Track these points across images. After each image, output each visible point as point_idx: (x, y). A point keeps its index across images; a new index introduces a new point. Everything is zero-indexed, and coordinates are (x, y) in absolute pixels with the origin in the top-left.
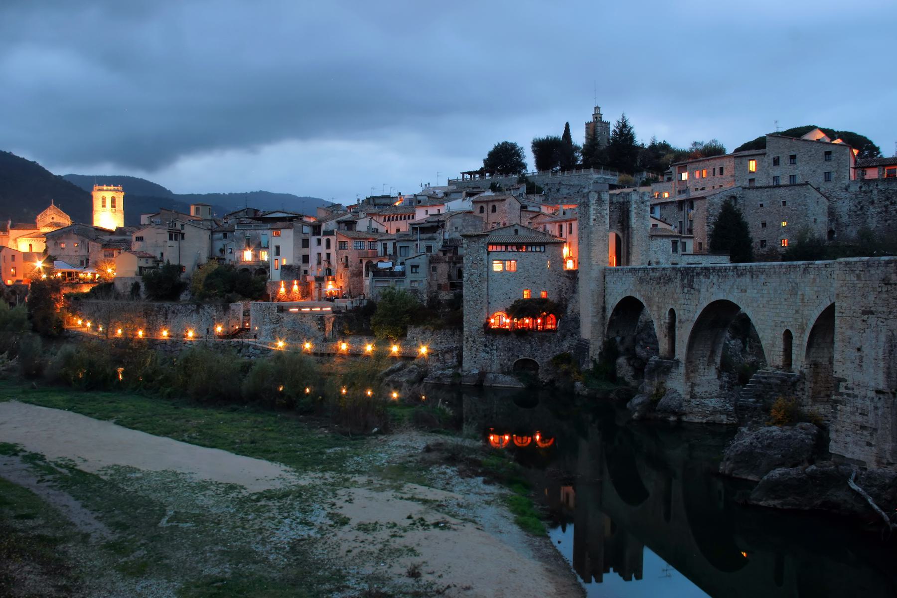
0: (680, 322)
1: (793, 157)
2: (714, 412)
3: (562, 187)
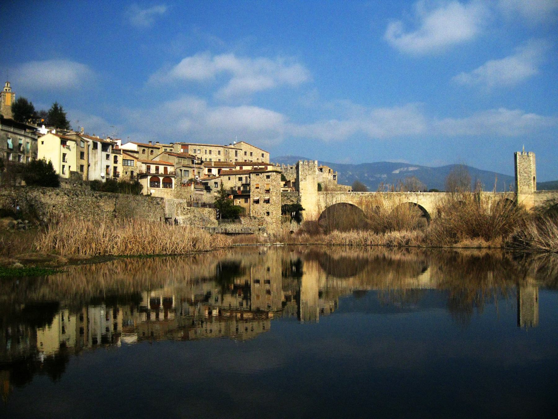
1: (251, 153)
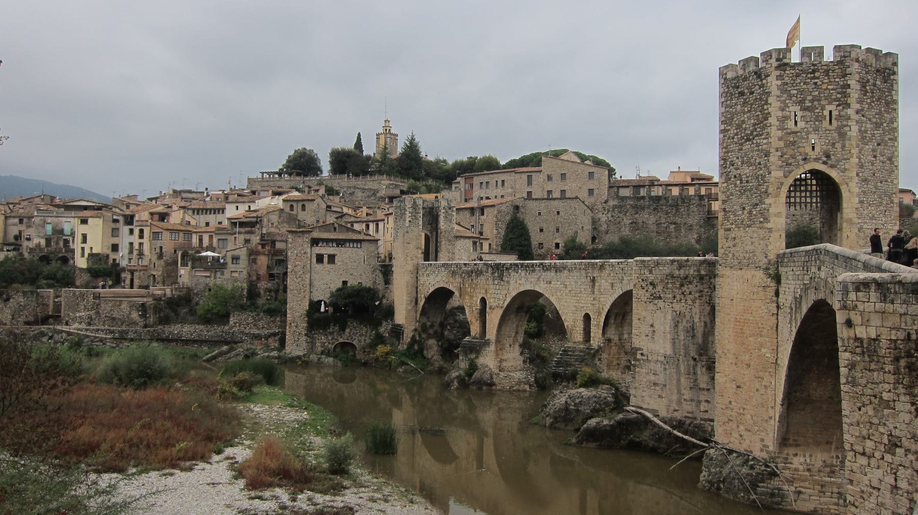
0: (490, 308)
1: (563, 176)
2: (519, 382)
3: (357, 191)
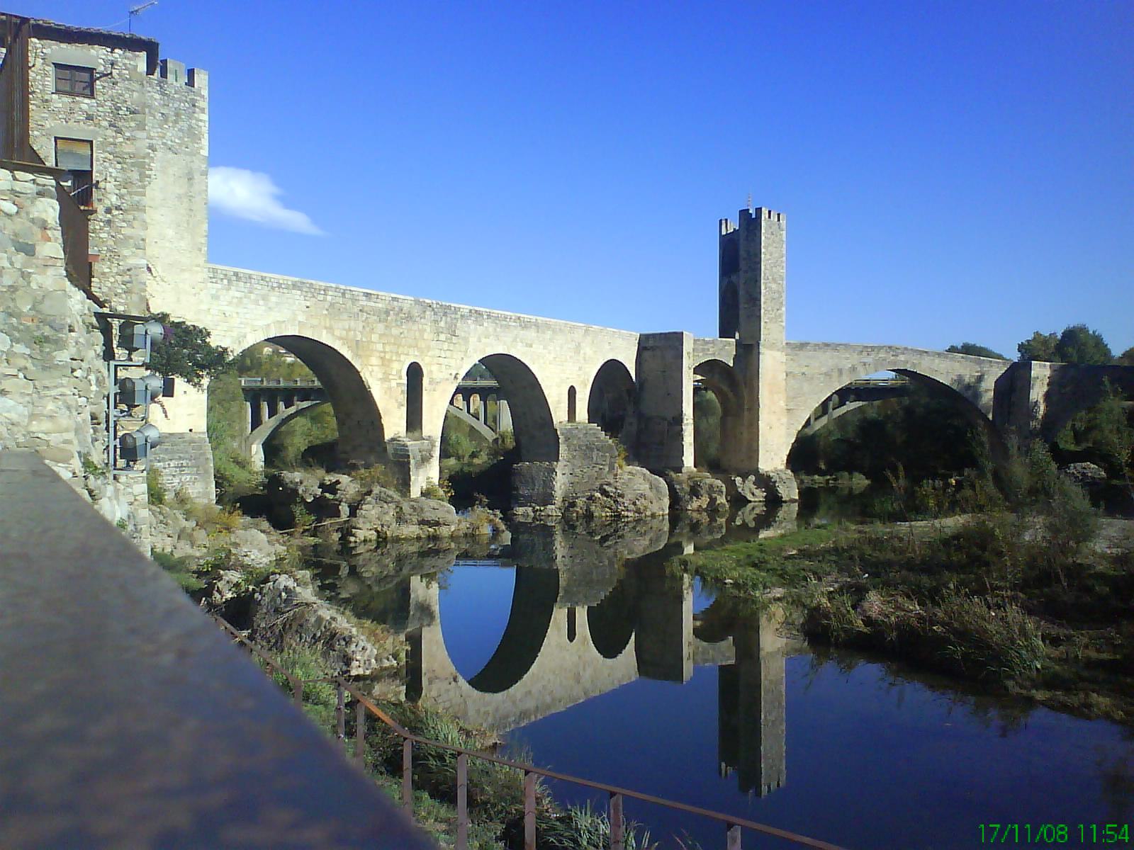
0: (431, 383)
